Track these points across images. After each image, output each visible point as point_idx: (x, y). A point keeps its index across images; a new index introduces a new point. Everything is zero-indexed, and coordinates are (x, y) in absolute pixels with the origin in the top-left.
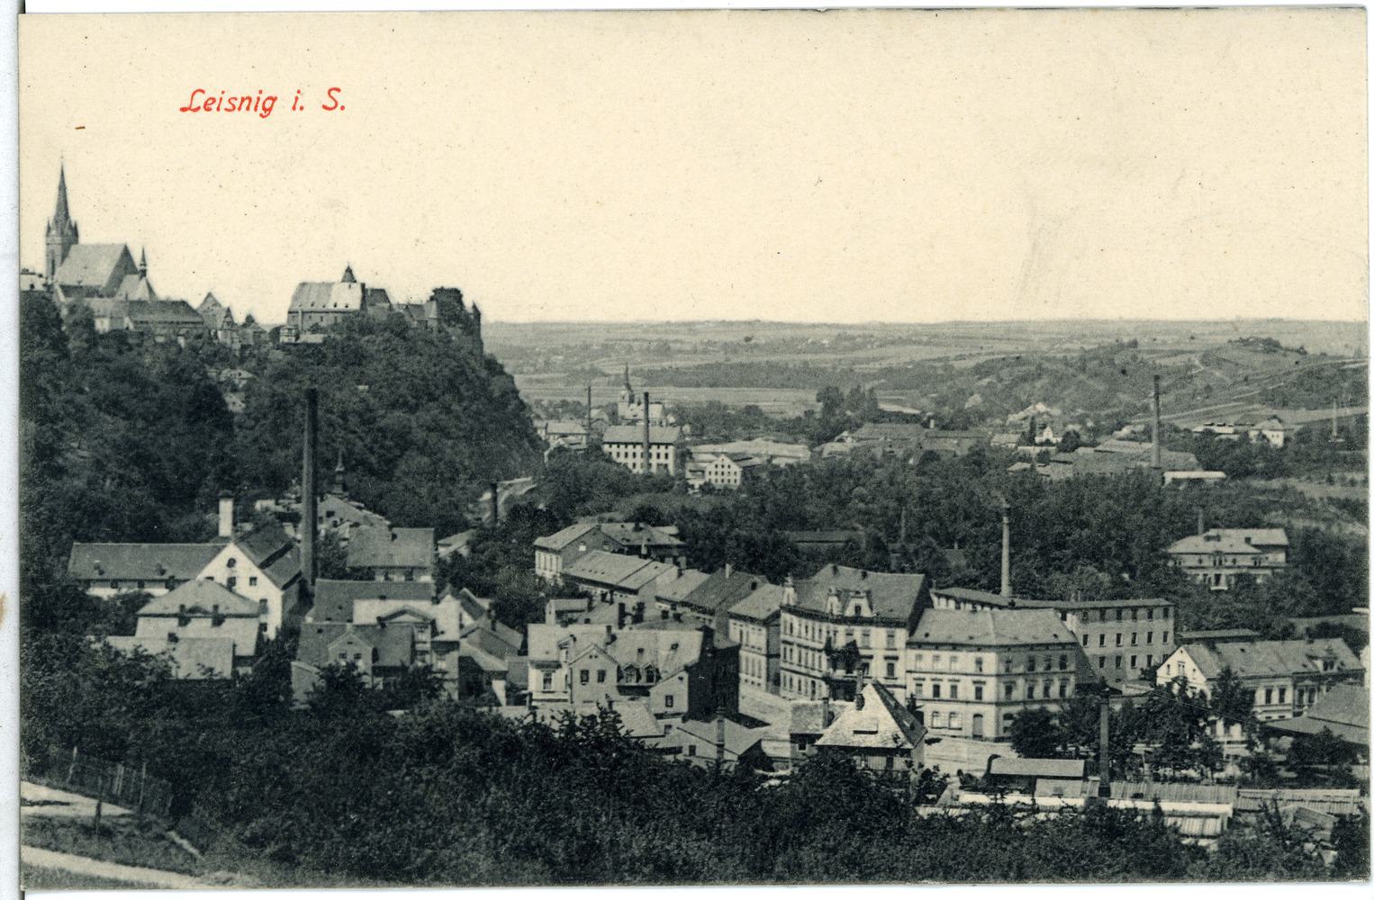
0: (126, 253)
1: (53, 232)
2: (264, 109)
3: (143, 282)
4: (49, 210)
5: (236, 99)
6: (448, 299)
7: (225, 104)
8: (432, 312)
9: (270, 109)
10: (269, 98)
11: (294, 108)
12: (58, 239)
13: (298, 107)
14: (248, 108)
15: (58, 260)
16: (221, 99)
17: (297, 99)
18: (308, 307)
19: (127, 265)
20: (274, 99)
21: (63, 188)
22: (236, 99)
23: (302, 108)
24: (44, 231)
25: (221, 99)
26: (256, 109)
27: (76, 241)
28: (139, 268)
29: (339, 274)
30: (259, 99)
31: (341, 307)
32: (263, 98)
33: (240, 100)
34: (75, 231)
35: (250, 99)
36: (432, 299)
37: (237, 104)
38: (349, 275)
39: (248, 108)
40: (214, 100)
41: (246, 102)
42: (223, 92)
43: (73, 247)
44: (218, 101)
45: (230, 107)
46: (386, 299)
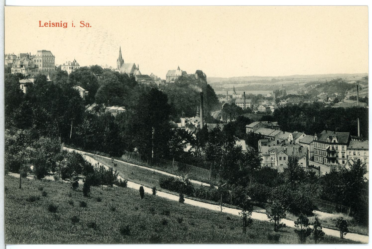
0: (134, 66)
1: (119, 61)
3: (138, 71)
4: (117, 57)
6: (200, 74)
8: (196, 76)
12: (120, 62)
15: (120, 66)
18: (170, 75)
19: (134, 68)
21: (120, 51)
24: (117, 61)
27: (124, 63)
28: (137, 68)
29: (177, 68)
31: (178, 75)
34: (123, 61)
36: (196, 73)
38: (179, 68)
43: (123, 64)
46: (186, 73)
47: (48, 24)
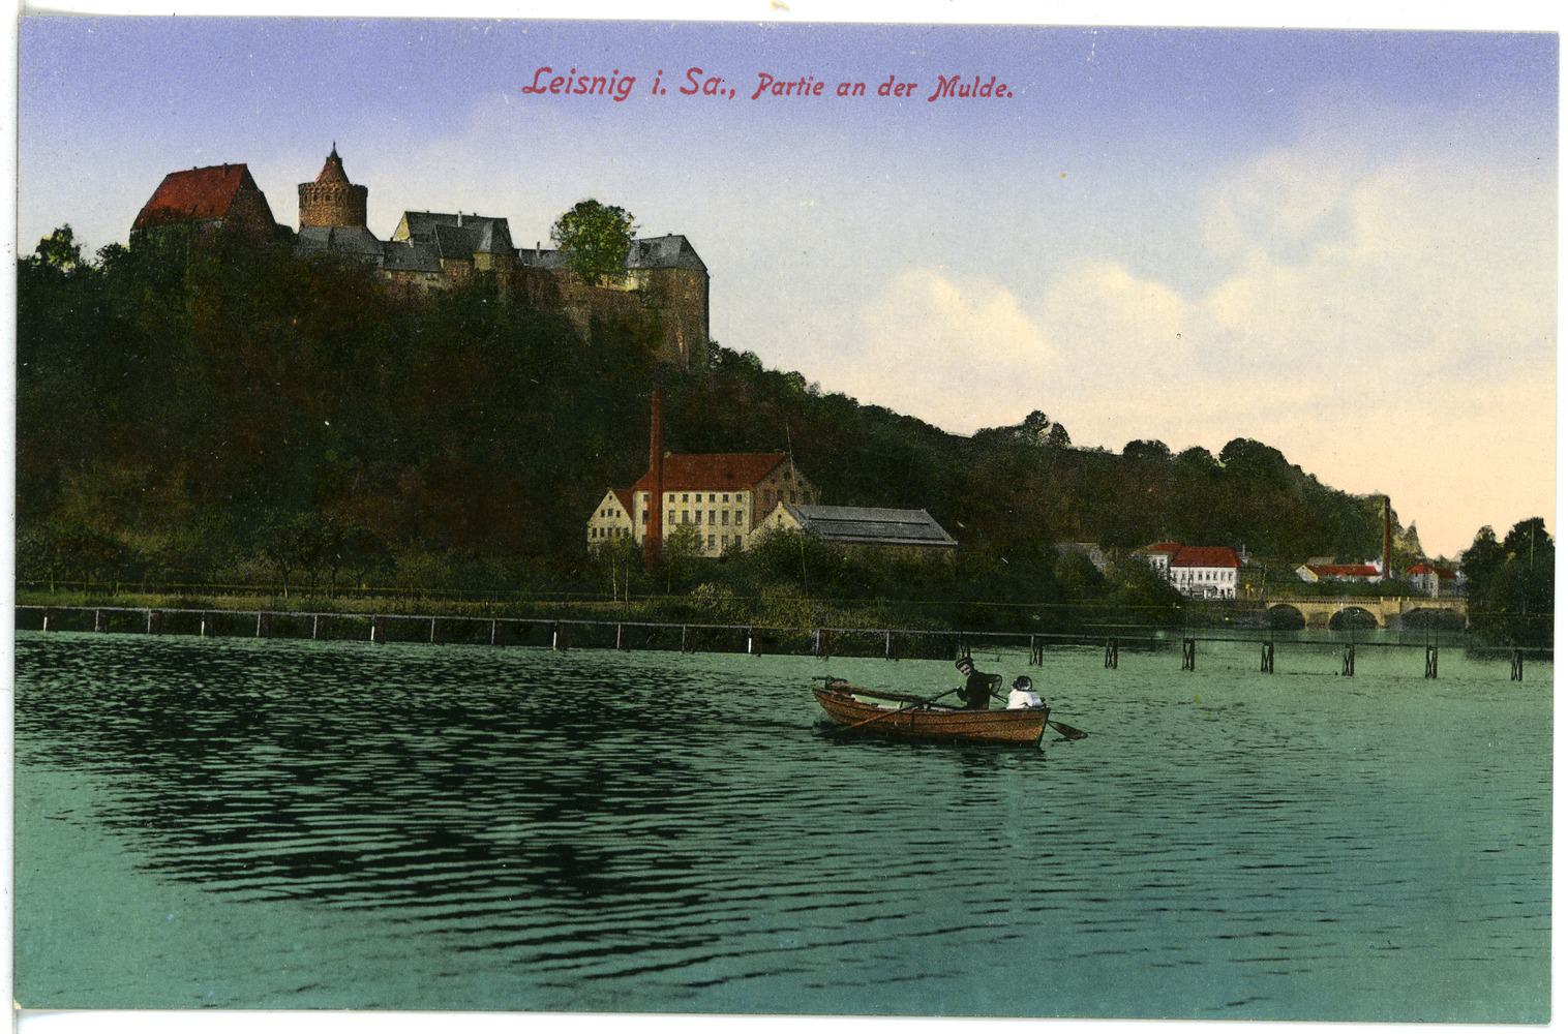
2: (621, 91)
5: (587, 79)
7: (575, 85)
9: (629, 89)
10: (627, 79)
11: (655, 92)
13: (659, 91)
14: (601, 92)
16: (571, 80)
17: (658, 81)
20: (632, 80)
22: (587, 79)
23: (663, 92)
25: (571, 80)
26: (610, 92)
30: (613, 80)
32: (619, 78)
33: (592, 82)
35: (604, 80)
37: (589, 84)
39: (601, 92)
40: (562, 80)
41: (600, 83)
42: (573, 71)
44: (567, 81)
45: (580, 88)
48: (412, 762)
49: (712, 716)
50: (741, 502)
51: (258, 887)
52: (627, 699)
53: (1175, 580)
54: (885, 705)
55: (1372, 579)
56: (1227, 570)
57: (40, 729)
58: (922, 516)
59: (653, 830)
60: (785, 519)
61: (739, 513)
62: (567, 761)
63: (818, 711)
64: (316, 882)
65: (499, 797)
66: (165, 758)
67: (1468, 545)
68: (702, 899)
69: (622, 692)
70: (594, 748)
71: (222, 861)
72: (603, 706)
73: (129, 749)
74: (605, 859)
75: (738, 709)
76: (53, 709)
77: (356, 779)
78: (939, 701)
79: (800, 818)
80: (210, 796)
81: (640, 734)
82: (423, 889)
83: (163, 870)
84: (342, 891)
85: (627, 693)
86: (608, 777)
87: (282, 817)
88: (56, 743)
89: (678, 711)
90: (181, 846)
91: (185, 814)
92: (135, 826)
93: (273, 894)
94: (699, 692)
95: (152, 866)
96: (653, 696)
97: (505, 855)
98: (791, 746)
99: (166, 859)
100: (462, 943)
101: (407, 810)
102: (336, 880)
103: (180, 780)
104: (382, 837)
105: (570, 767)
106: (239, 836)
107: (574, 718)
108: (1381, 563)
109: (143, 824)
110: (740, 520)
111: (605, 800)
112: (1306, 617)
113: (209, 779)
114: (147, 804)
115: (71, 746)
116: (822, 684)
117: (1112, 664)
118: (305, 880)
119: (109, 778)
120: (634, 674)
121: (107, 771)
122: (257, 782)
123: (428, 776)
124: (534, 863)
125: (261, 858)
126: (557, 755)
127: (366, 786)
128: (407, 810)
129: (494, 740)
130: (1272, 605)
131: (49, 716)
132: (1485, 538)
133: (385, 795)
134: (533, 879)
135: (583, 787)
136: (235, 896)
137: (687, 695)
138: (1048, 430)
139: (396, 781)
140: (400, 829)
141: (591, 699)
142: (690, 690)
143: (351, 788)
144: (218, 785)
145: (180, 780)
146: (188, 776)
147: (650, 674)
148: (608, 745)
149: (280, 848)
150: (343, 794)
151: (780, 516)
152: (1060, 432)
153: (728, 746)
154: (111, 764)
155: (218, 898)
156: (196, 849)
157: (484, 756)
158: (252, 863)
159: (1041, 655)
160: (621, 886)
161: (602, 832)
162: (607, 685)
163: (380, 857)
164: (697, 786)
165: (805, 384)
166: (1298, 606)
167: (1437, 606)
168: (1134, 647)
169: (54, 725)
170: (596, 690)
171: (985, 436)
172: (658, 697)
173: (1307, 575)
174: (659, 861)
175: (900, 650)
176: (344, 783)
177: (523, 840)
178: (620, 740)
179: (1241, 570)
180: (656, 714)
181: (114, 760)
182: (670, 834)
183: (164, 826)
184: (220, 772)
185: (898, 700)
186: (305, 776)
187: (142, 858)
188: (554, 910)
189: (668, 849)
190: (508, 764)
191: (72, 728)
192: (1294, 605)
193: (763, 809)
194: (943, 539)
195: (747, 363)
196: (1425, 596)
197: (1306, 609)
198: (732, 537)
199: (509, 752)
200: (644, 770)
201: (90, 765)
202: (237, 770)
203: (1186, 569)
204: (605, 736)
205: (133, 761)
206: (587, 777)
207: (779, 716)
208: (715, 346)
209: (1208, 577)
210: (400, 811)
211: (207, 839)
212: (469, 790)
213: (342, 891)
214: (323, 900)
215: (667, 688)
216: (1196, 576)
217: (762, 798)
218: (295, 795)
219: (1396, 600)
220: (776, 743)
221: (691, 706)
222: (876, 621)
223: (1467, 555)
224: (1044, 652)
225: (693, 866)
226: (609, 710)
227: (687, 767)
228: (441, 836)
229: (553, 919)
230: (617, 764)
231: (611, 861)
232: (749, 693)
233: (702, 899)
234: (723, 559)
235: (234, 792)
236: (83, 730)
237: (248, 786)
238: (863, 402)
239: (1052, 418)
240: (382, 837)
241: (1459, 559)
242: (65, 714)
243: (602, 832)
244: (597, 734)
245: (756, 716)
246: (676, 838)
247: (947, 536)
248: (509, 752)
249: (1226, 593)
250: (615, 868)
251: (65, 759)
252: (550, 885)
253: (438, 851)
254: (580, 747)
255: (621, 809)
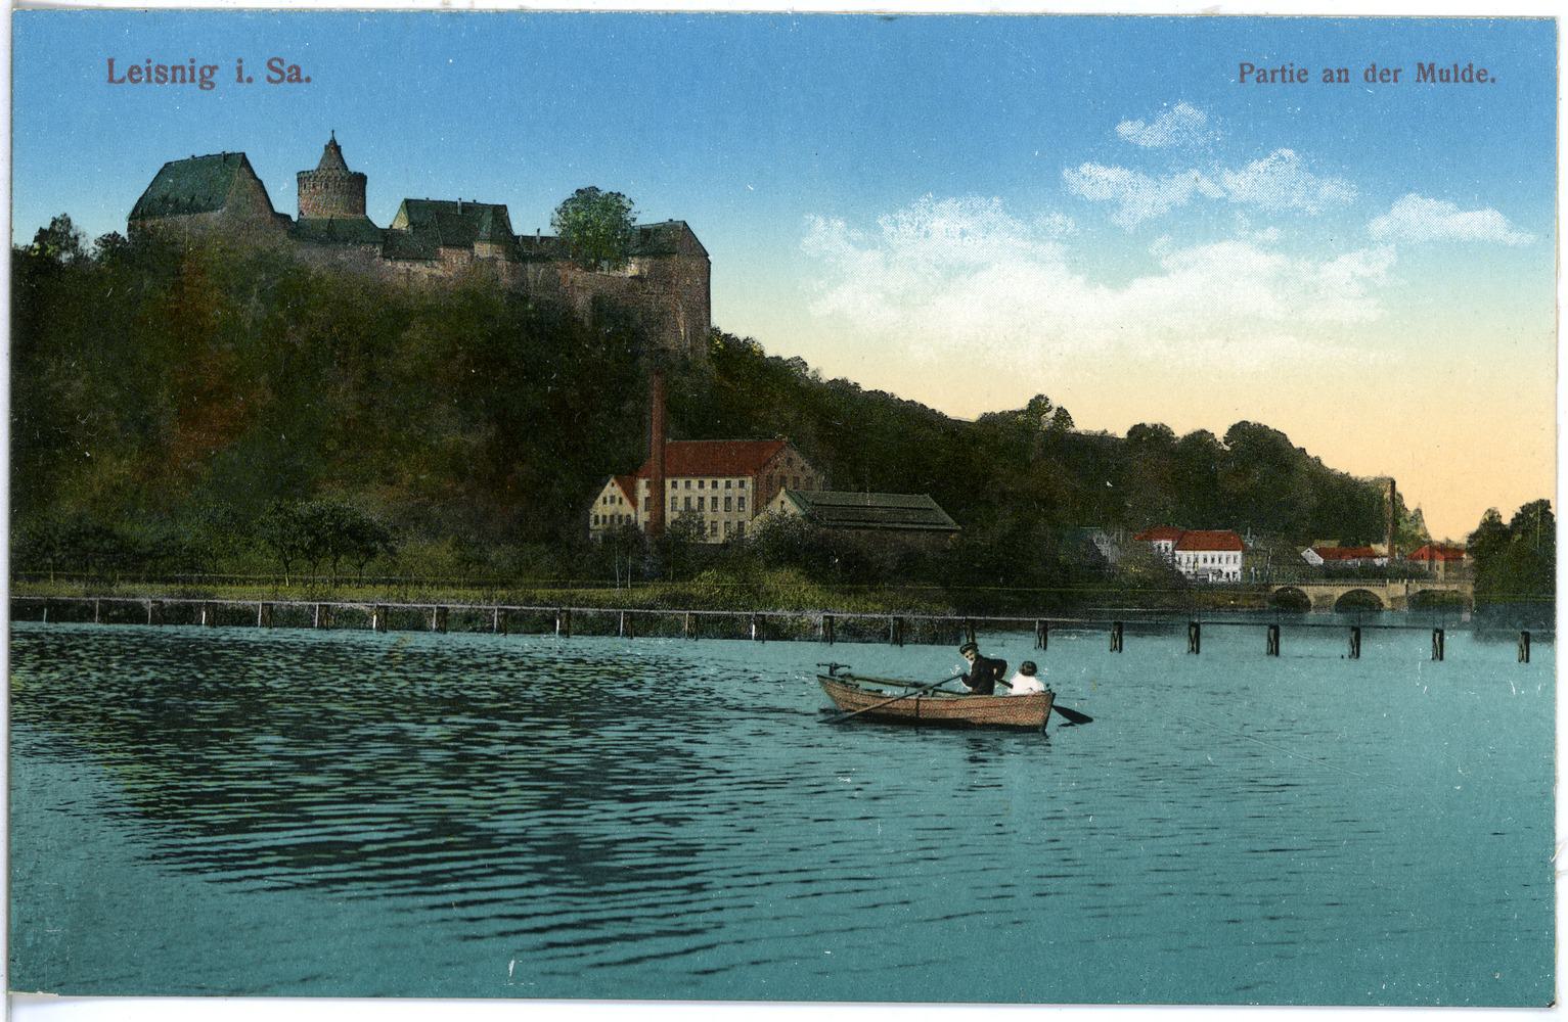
47: (140, 71)
48: (415, 751)
49: (716, 703)
50: (743, 488)
51: (260, 877)
52: (629, 686)
53: (1180, 563)
54: (888, 691)
55: (1378, 562)
56: (1232, 553)
57: (40, 721)
58: (926, 501)
59: (657, 818)
60: (784, 505)
61: (741, 499)
62: (570, 749)
63: (819, 699)
64: (318, 872)
65: (502, 785)
66: (167, 749)
67: (1474, 527)
68: (707, 886)
69: (625, 679)
70: (597, 736)
71: (226, 852)
72: (608, 694)
73: (130, 740)
74: (610, 847)
75: (742, 696)
76: (52, 700)
77: (359, 768)
78: (944, 686)
79: (804, 805)
80: (211, 786)
81: (642, 721)
82: (429, 879)
83: (165, 861)
84: (344, 881)
85: (631, 681)
86: (612, 764)
87: (286, 807)
88: (55, 734)
89: (683, 698)
90: (183, 837)
91: (188, 804)
92: (136, 817)
93: (277, 884)
94: (703, 679)
95: (154, 857)
96: (657, 683)
97: (510, 843)
98: (796, 732)
99: (168, 850)
100: (464, 933)
101: (410, 799)
102: (339, 870)
103: (182, 770)
104: (386, 827)
105: (575, 755)
106: (241, 827)
107: (577, 707)
108: (1387, 546)
109: (146, 815)
110: (743, 507)
111: (609, 788)
112: (1312, 598)
113: (207, 769)
114: (149, 794)
115: (72, 737)
116: (826, 671)
117: (1117, 646)
118: (307, 870)
119: (110, 769)
120: (638, 660)
121: (109, 762)
122: (259, 772)
123: (432, 764)
124: (539, 851)
125: (265, 848)
126: (560, 743)
127: (369, 775)
128: (410, 799)
129: (496, 728)
130: (1277, 588)
131: (49, 708)
132: (1491, 523)
133: (387, 784)
134: (538, 867)
135: (585, 775)
136: (235, 886)
137: (691, 683)
138: (1051, 415)
139: (401, 770)
140: (402, 818)
141: (595, 686)
142: (693, 677)
143: (353, 777)
144: (220, 776)
145: (182, 770)
146: (190, 767)
147: (653, 661)
148: (611, 733)
149: (282, 839)
150: (346, 784)
151: (783, 502)
152: (1063, 416)
153: (732, 733)
154: (111, 755)
155: (221, 888)
156: (198, 840)
157: (487, 745)
158: (255, 853)
159: (1046, 639)
160: (631, 874)
161: (603, 820)
162: (611, 673)
163: (383, 846)
164: (700, 773)
165: (807, 369)
166: (1304, 589)
167: (1444, 588)
168: (1141, 630)
169: (55, 717)
170: (598, 678)
171: (988, 420)
172: (662, 684)
173: (1314, 558)
174: (663, 848)
175: (899, 635)
176: (347, 773)
177: (527, 828)
178: (623, 728)
179: (1247, 553)
180: (660, 702)
181: (115, 751)
182: (674, 822)
183: (166, 817)
184: (221, 762)
185: (903, 686)
186: (309, 766)
187: (141, 849)
188: (558, 898)
189: (672, 836)
190: (511, 752)
191: (73, 719)
192: (1301, 588)
193: (768, 796)
194: (944, 524)
195: (750, 350)
196: (1433, 578)
197: (1311, 592)
198: (734, 525)
199: (513, 741)
200: (647, 758)
201: (91, 757)
202: (239, 760)
203: (1191, 553)
204: (608, 724)
205: (134, 752)
206: (593, 765)
207: (780, 703)
208: (716, 331)
209: (1213, 560)
210: (403, 800)
211: (210, 829)
212: (472, 778)
213: (344, 881)
214: (326, 889)
215: (671, 675)
216: (1201, 560)
217: (762, 785)
218: (298, 785)
219: (1403, 581)
220: (780, 730)
221: (694, 693)
222: (879, 606)
223: (1473, 537)
224: (1049, 638)
225: (698, 854)
226: (612, 698)
227: (691, 754)
228: (445, 825)
229: (558, 907)
230: (621, 752)
231: (614, 849)
232: (754, 680)
233: (707, 886)
234: (725, 545)
235: (236, 782)
236: (83, 721)
237: (250, 777)
238: (866, 387)
239: (1055, 402)
240: (386, 827)
241: (1465, 541)
242: (64, 706)
243: (603, 820)
244: (599, 722)
245: (760, 703)
246: (680, 825)
247: (950, 520)
248: (513, 741)
249: (1231, 576)
250: (618, 856)
251: (65, 751)
252: (554, 873)
253: (442, 841)
254: (584, 734)
255: (626, 798)
